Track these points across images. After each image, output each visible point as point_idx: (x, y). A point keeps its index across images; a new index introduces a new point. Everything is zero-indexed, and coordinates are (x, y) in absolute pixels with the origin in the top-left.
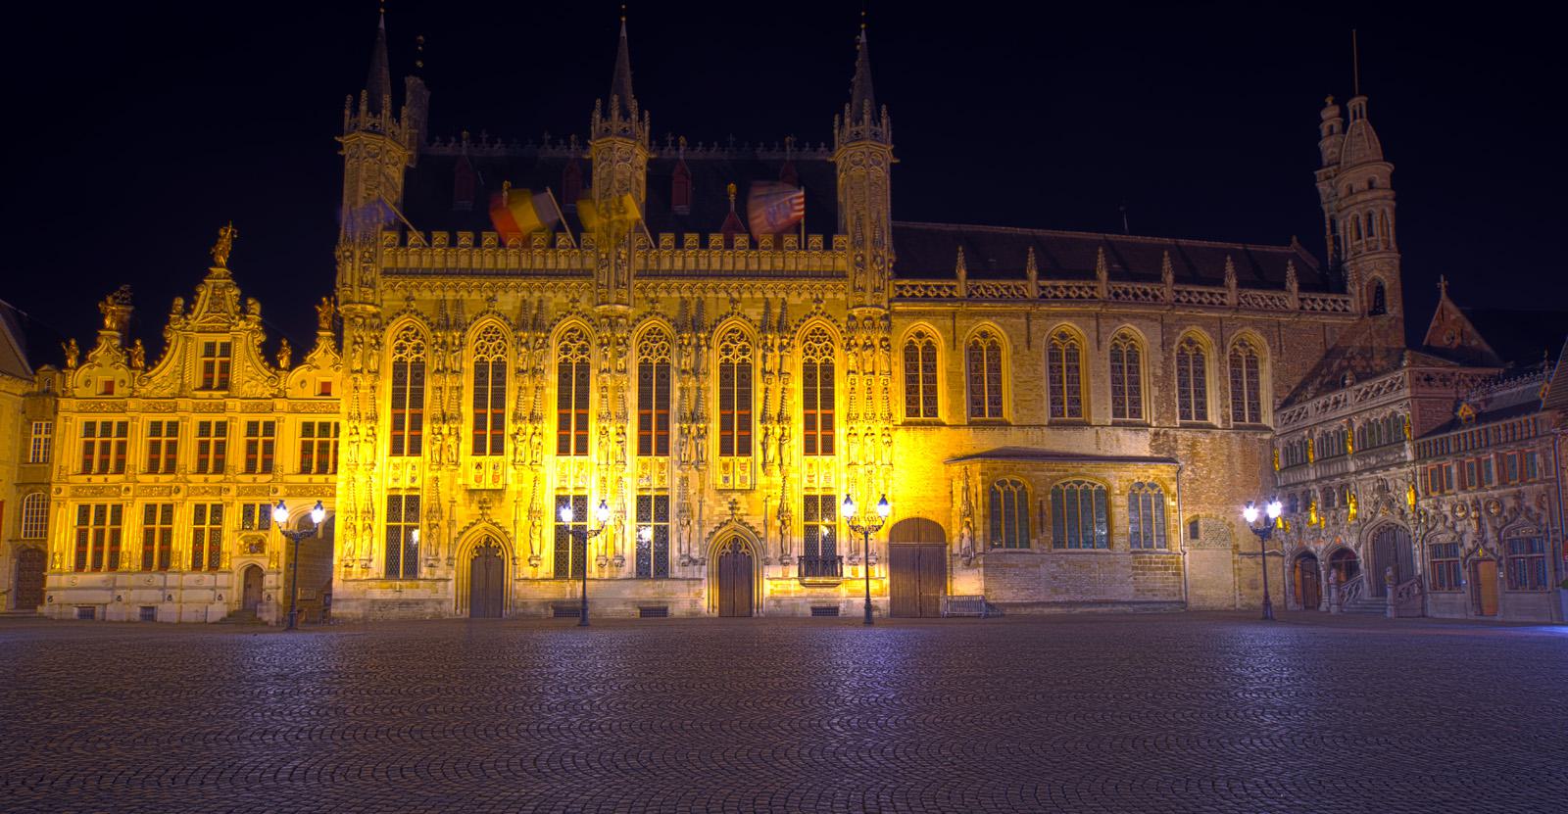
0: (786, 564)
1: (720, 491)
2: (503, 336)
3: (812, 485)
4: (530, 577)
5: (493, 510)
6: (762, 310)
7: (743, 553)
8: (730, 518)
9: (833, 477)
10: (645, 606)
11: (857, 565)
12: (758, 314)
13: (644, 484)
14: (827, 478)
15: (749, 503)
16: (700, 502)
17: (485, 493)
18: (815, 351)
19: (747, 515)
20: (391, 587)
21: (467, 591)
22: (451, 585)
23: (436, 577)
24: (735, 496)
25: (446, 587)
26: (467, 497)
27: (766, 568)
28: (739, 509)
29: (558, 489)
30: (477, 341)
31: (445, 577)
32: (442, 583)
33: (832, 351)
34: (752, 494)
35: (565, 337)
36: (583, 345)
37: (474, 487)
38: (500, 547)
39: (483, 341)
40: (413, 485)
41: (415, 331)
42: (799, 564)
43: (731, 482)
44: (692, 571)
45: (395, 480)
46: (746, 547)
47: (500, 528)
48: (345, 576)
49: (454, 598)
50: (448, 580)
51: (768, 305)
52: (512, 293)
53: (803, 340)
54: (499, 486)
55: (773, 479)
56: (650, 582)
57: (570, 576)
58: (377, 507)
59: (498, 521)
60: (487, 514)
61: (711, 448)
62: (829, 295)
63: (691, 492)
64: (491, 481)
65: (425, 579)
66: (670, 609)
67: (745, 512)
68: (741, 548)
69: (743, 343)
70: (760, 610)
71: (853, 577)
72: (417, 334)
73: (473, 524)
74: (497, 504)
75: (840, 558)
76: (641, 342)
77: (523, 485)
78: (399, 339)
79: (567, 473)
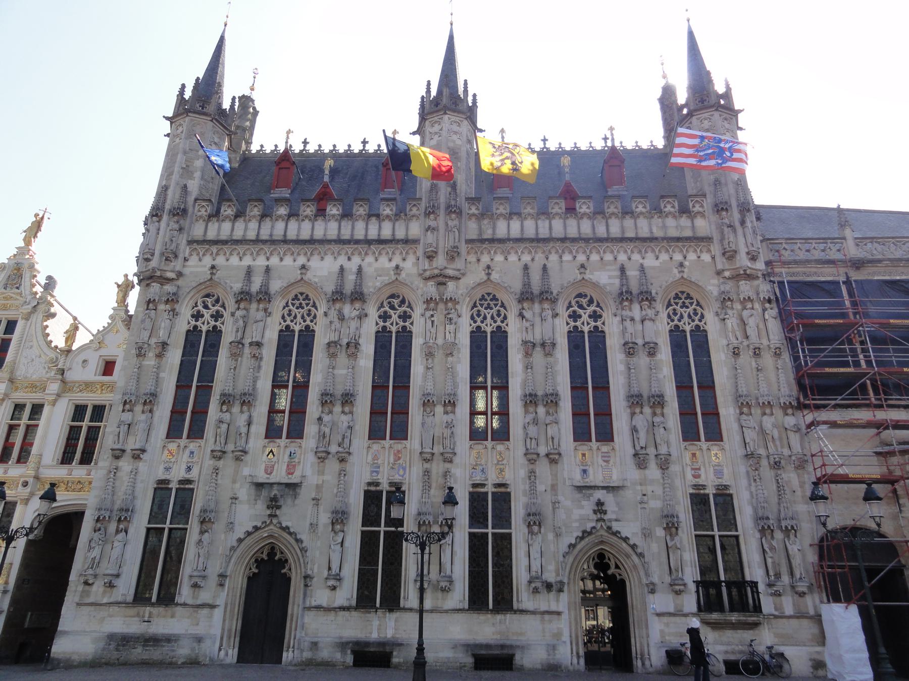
0: (678, 593)
1: (580, 488)
2: (314, 303)
3: (701, 481)
4: (325, 605)
5: (284, 508)
6: (618, 273)
7: (614, 575)
8: (593, 524)
9: (725, 471)
10: (483, 652)
11: (780, 595)
12: (610, 277)
13: (478, 479)
14: (719, 473)
15: (618, 504)
16: (554, 503)
17: (275, 487)
18: (682, 317)
19: (616, 520)
20: (138, 615)
21: (236, 624)
22: (218, 613)
23: (199, 602)
24: (599, 495)
25: (210, 617)
26: (253, 490)
27: (651, 596)
28: (605, 512)
29: (369, 484)
30: (284, 308)
31: (210, 602)
32: (205, 611)
33: (702, 316)
34: (621, 492)
35: (385, 304)
36: (405, 312)
37: (261, 480)
38: (286, 561)
39: (291, 307)
40: (188, 476)
41: (216, 297)
42: (697, 592)
43: (591, 477)
44: (546, 602)
45: (167, 469)
46: (617, 567)
47: (290, 534)
48: (81, 596)
49: (218, 633)
50: (212, 607)
51: (622, 270)
52: (329, 259)
53: (666, 303)
54: (294, 479)
55: (647, 472)
56: (489, 616)
57: (378, 605)
58: (138, 503)
59: (289, 524)
60: (276, 516)
61: (563, 431)
62: (692, 256)
63: (541, 488)
64: (284, 473)
65: (185, 605)
66: (518, 659)
67: (614, 517)
68: (608, 567)
69: (593, 308)
70: (647, 663)
71: (776, 613)
72: (217, 301)
73: (256, 528)
74: (289, 501)
75: (754, 585)
76: (472, 308)
77: (325, 478)
78: (196, 306)
79: (380, 462)
